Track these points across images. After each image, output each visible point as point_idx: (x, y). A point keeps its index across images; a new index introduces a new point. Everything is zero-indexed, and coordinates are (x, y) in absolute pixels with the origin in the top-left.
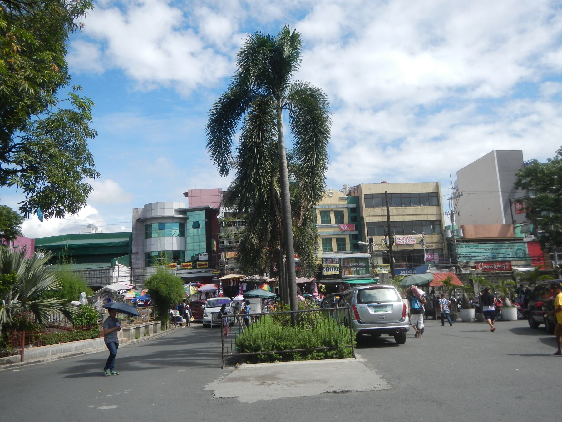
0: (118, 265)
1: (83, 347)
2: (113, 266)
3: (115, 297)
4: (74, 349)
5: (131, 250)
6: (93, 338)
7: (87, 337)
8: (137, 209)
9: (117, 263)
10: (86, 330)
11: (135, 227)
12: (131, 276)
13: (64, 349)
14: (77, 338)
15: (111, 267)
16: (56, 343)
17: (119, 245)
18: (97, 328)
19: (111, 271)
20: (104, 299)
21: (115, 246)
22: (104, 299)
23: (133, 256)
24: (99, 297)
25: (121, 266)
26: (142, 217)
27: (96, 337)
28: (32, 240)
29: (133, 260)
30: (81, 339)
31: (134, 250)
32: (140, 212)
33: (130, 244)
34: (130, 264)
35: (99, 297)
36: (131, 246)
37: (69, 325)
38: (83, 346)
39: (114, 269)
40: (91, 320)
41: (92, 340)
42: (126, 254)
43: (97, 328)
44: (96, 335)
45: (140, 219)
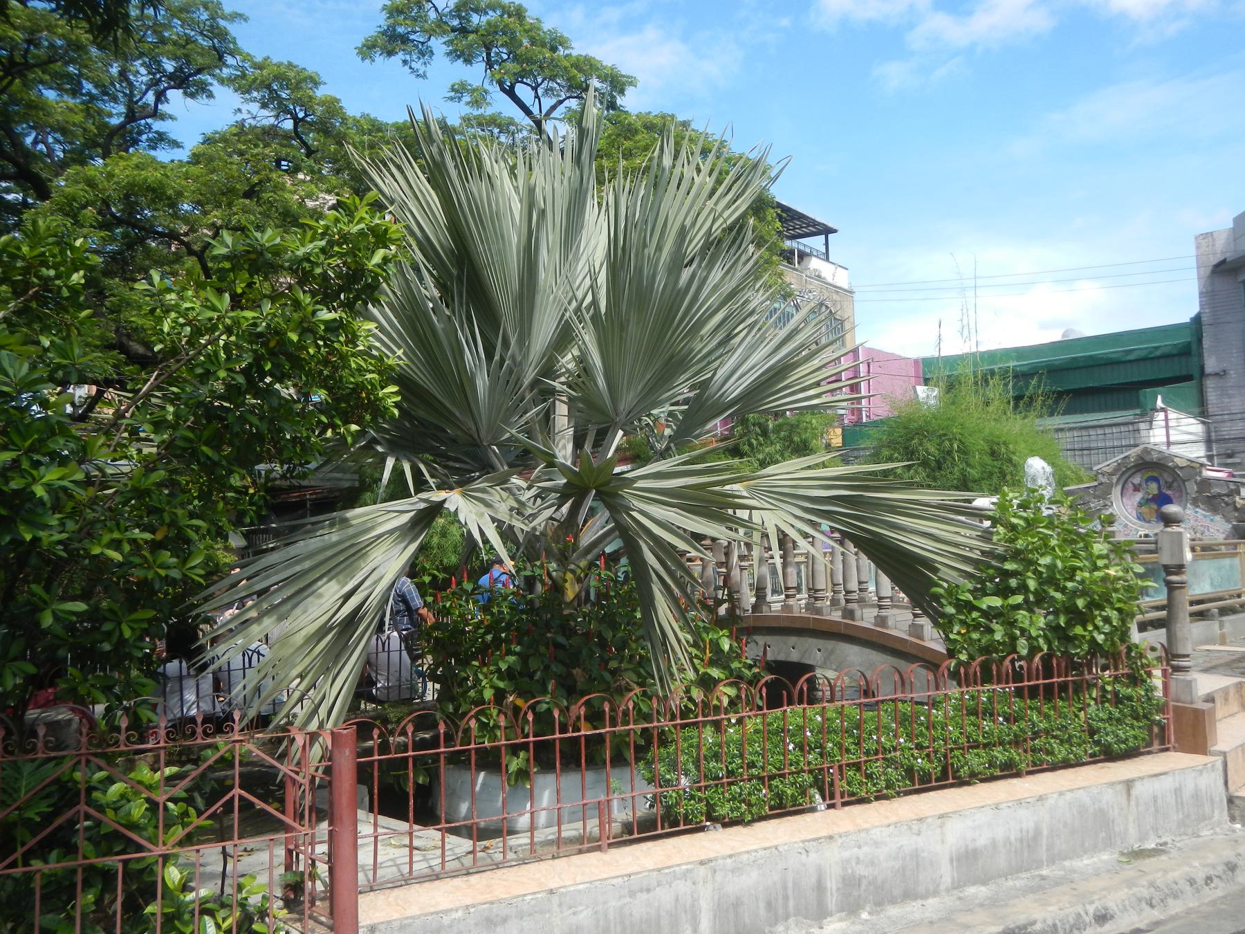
0: (1162, 410)
1: (1027, 852)
2: (1147, 413)
3: (1192, 487)
4: (946, 874)
5: (1202, 368)
6: (1109, 755)
7: (1061, 752)
8: (1208, 236)
9: (1160, 403)
10: (1049, 693)
11: (1209, 295)
12: (1209, 442)
13: (850, 882)
14: (976, 760)
15: (1143, 415)
16: (783, 808)
17: (1158, 353)
18: (1135, 680)
19: (1142, 426)
20: (1139, 496)
21: (1144, 359)
22: (1139, 496)
23: (1210, 384)
24: (1116, 491)
25: (1172, 415)
26: (1230, 256)
27: (1131, 754)
28: (916, 361)
29: (1212, 396)
30: (1010, 771)
31: (1211, 364)
32: (1220, 244)
33: (1194, 347)
34: (1202, 411)
35: (1116, 491)
36: (1201, 355)
37: (933, 639)
38: (1030, 841)
39: (1151, 422)
40: (1081, 618)
41: (1092, 782)
42: (1188, 378)
43: (1135, 680)
44: (1129, 732)
45: (1223, 262)
